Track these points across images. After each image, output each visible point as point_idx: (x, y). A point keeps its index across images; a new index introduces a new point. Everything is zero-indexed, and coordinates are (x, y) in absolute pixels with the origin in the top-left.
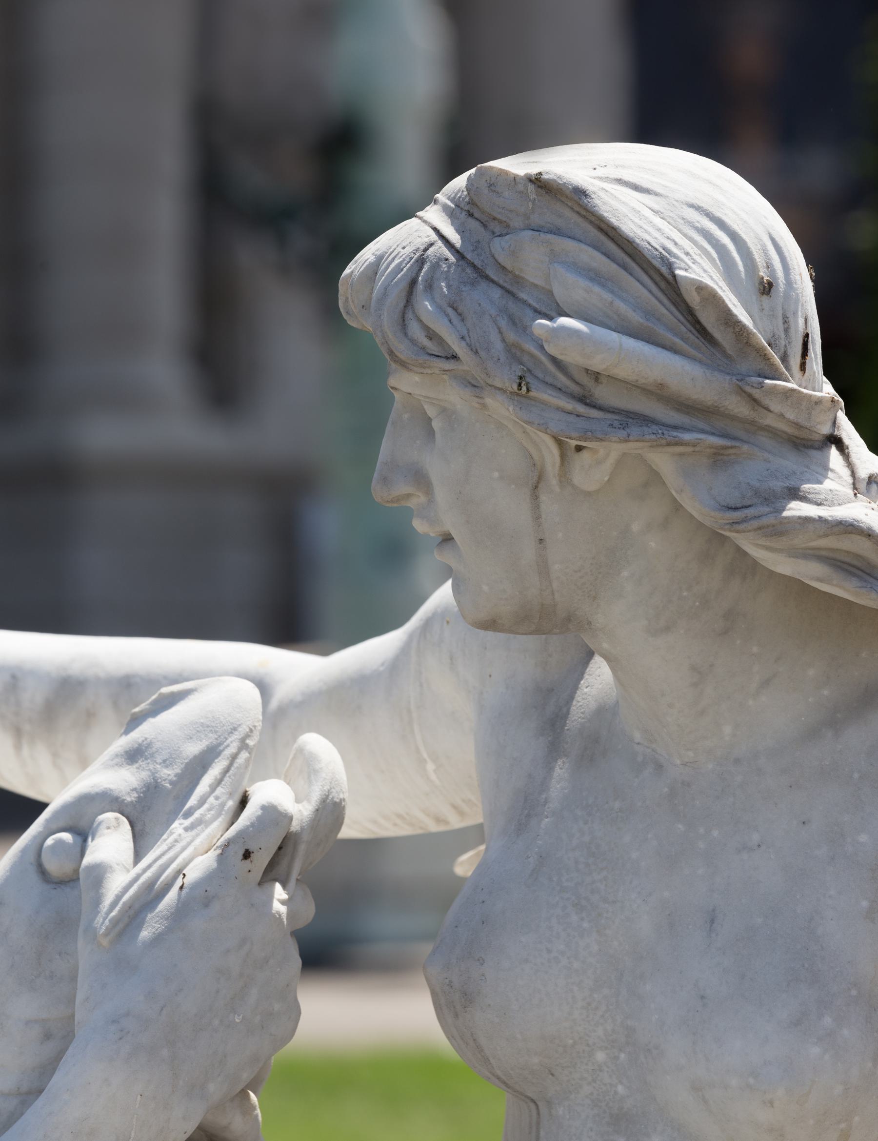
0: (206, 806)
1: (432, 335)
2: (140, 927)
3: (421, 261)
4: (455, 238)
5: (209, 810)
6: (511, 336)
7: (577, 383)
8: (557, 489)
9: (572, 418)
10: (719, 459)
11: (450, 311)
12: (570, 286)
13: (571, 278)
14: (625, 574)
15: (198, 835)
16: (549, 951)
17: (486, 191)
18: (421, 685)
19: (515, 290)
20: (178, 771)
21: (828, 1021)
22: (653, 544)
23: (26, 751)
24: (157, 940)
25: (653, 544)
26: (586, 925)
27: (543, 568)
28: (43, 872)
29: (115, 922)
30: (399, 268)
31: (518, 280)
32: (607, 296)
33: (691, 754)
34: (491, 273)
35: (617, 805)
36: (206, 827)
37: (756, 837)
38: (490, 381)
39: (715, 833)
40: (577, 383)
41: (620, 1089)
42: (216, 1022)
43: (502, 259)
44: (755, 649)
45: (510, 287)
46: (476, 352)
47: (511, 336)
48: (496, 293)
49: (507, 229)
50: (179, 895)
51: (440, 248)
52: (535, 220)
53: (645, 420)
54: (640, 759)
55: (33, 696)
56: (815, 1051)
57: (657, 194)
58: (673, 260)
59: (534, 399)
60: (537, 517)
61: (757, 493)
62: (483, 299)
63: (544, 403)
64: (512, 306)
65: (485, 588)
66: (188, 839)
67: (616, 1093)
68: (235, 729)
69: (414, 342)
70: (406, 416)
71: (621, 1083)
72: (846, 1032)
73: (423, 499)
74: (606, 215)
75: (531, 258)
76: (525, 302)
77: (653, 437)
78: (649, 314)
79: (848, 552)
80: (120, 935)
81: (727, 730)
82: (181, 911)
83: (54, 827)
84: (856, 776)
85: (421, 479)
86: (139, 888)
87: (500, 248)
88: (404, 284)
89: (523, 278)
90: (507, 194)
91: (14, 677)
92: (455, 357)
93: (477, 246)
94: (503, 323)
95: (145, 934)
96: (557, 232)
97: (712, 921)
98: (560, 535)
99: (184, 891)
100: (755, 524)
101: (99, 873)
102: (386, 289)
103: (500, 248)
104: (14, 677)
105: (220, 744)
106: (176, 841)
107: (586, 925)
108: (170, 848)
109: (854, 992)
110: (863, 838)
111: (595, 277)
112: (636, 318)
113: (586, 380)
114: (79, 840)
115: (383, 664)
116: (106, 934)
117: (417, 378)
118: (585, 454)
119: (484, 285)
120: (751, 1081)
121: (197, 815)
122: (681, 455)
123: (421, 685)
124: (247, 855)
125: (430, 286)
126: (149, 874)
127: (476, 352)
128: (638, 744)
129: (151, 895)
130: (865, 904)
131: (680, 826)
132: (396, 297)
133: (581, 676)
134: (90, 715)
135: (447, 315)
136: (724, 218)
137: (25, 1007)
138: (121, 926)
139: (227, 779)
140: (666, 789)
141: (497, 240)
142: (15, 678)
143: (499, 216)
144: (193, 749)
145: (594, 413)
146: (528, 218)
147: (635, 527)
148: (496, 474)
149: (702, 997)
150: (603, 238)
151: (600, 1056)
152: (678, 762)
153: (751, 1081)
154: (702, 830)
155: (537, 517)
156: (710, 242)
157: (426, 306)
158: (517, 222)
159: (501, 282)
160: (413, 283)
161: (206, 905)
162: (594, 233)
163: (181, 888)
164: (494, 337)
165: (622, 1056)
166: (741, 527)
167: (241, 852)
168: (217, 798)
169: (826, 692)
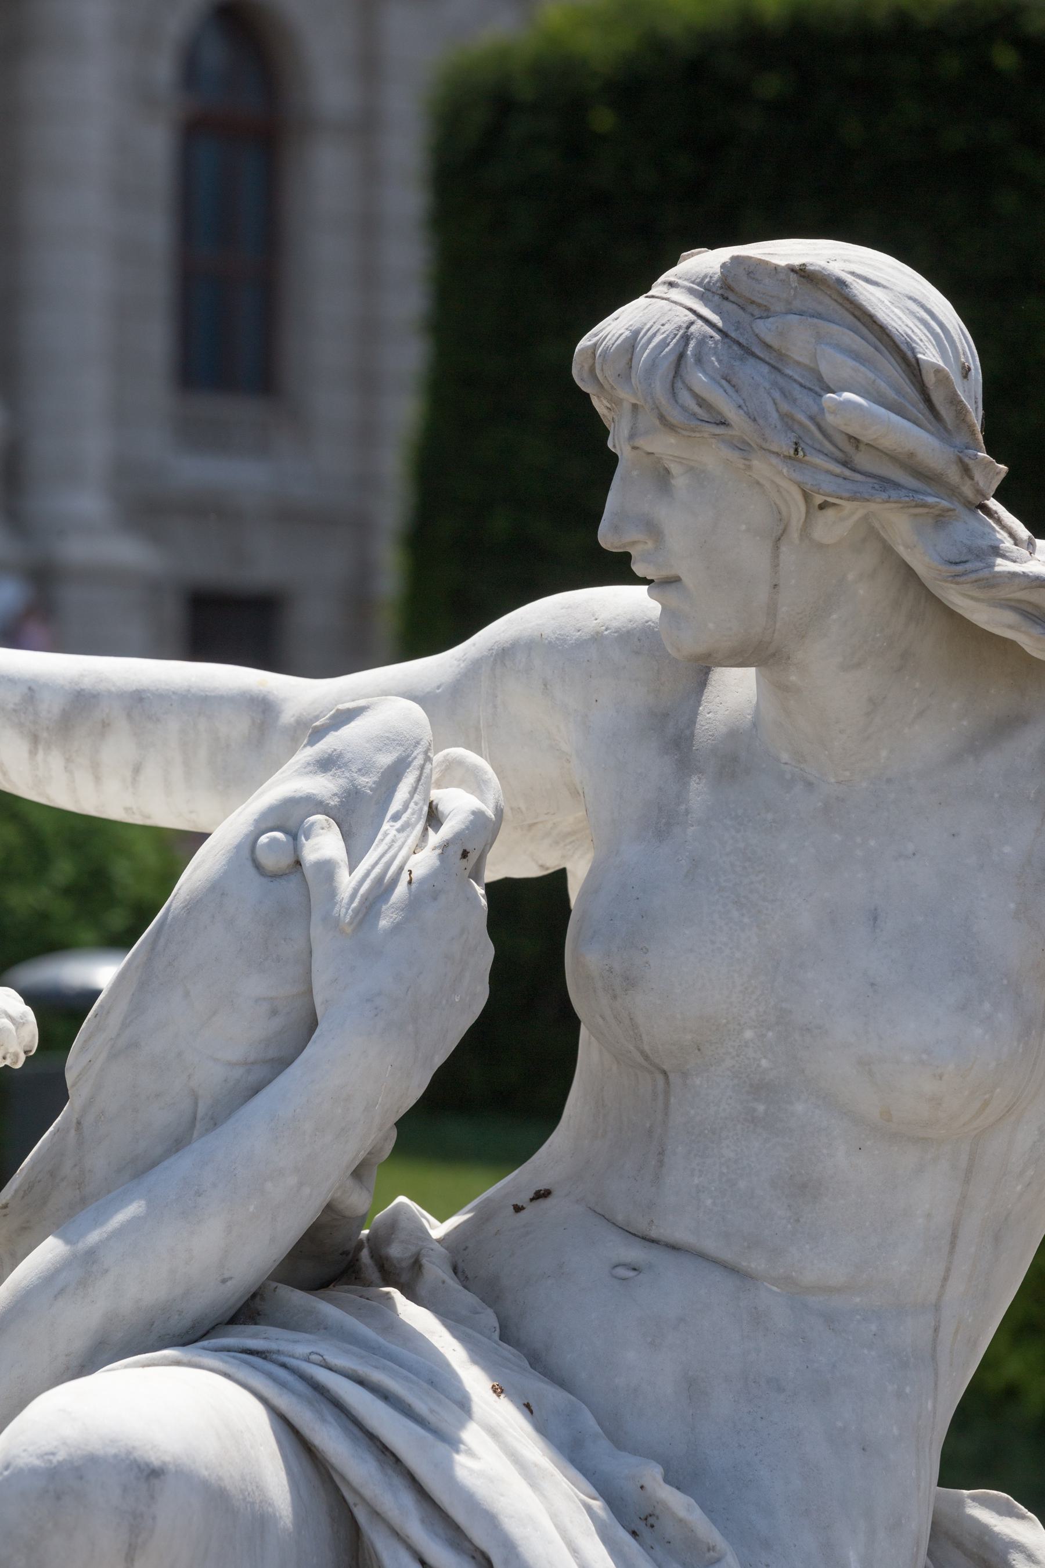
0: (409, 811)
1: (701, 402)
2: (378, 916)
3: (686, 338)
4: (715, 318)
5: (413, 814)
6: (785, 407)
7: (841, 450)
8: (797, 541)
9: (840, 481)
10: (941, 519)
11: (724, 382)
12: (833, 364)
13: (840, 357)
14: (834, 616)
15: (408, 836)
16: (713, 942)
17: (745, 278)
18: (495, 707)
19: (779, 365)
20: (375, 779)
21: (987, 1006)
22: (861, 592)
23: (40, 755)
24: (396, 929)
25: (861, 592)
26: (746, 920)
27: (772, 610)
28: (257, 866)
29: (357, 912)
30: (664, 343)
31: (781, 356)
32: (871, 375)
33: (848, 774)
34: (757, 351)
35: (770, 816)
36: (413, 829)
37: (911, 847)
38: (765, 445)
39: (872, 843)
40: (841, 450)
41: (764, 1063)
42: (444, 1002)
43: (769, 339)
44: (917, 685)
45: (775, 361)
46: (755, 420)
47: (785, 407)
48: (766, 369)
49: (766, 313)
50: (409, 889)
51: (699, 326)
52: (797, 304)
53: (897, 486)
54: (788, 776)
55: (50, 707)
56: (979, 1031)
57: (884, 287)
58: (914, 345)
59: (807, 463)
60: (775, 566)
61: (970, 550)
62: (752, 373)
63: (815, 467)
64: (781, 380)
65: (711, 626)
66: (402, 840)
67: (759, 1066)
68: (418, 743)
69: (684, 409)
70: (635, 473)
71: (765, 1057)
72: (1000, 1015)
73: (650, 545)
74: (864, 303)
75: (799, 341)
76: (790, 377)
77: (907, 499)
78: (898, 391)
79: (1029, 603)
80: (361, 923)
81: (884, 753)
82: (414, 903)
83: (263, 826)
84: (996, 795)
85: (654, 530)
86: (373, 882)
87: (765, 329)
88: (673, 358)
89: (787, 356)
90: (767, 281)
91: (30, 688)
92: (724, 423)
93: (738, 326)
94: (777, 395)
95: (384, 923)
96: (819, 316)
97: (875, 919)
98: (793, 582)
99: (414, 886)
100: (974, 576)
101: (327, 868)
102: (654, 361)
103: (765, 329)
104: (30, 688)
105: (408, 756)
106: (393, 841)
107: (746, 920)
108: (390, 847)
109: (1005, 982)
110: (1007, 849)
111: (856, 356)
112: (891, 394)
113: (849, 448)
114: (290, 838)
115: (438, 687)
116: (350, 923)
117: (673, 441)
118: (830, 513)
119: (751, 361)
120: (924, 1057)
121: (404, 817)
122: (916, 515)
123: (495, 707)
124: (465, 854)
125: (699, 360)
126: (377, 870)
127: (755, 420)
128: (786, 764)
129: (382, 889)
130: (1012, 906)
131: (836, 836)
132: (665, 367)
134: (105, 725)
135: (722, 386)
136: (933, 310)
137: (256, 986)
138: (361, 916)
139: (420, 787)
140: (820, 804)
141: (760, 322)
142: (31, 691)
143: (760, 301)
144: (385, 759)
145: (858, 477)
146: (790, 303)
147: (851, 577)
148: (743, 527)
149: (872, 984)
150: (858, 324)
151: (749, 1034)
152: (833, 780)
153: (924, 1057)
154: (859, 840)
155: (775, 566)
156: (929, 331)
157: (699, 379)
158: (779, 307)
159: (767, 359)
160: (681, 356)
161: (435, 898)
162: (850, 318)
163: (410, 882)
164: (770, 407)
165: (770, 1034)
166: (962, 579)
167: (460, 852)
168: (416, 804)
169: (965, 723)
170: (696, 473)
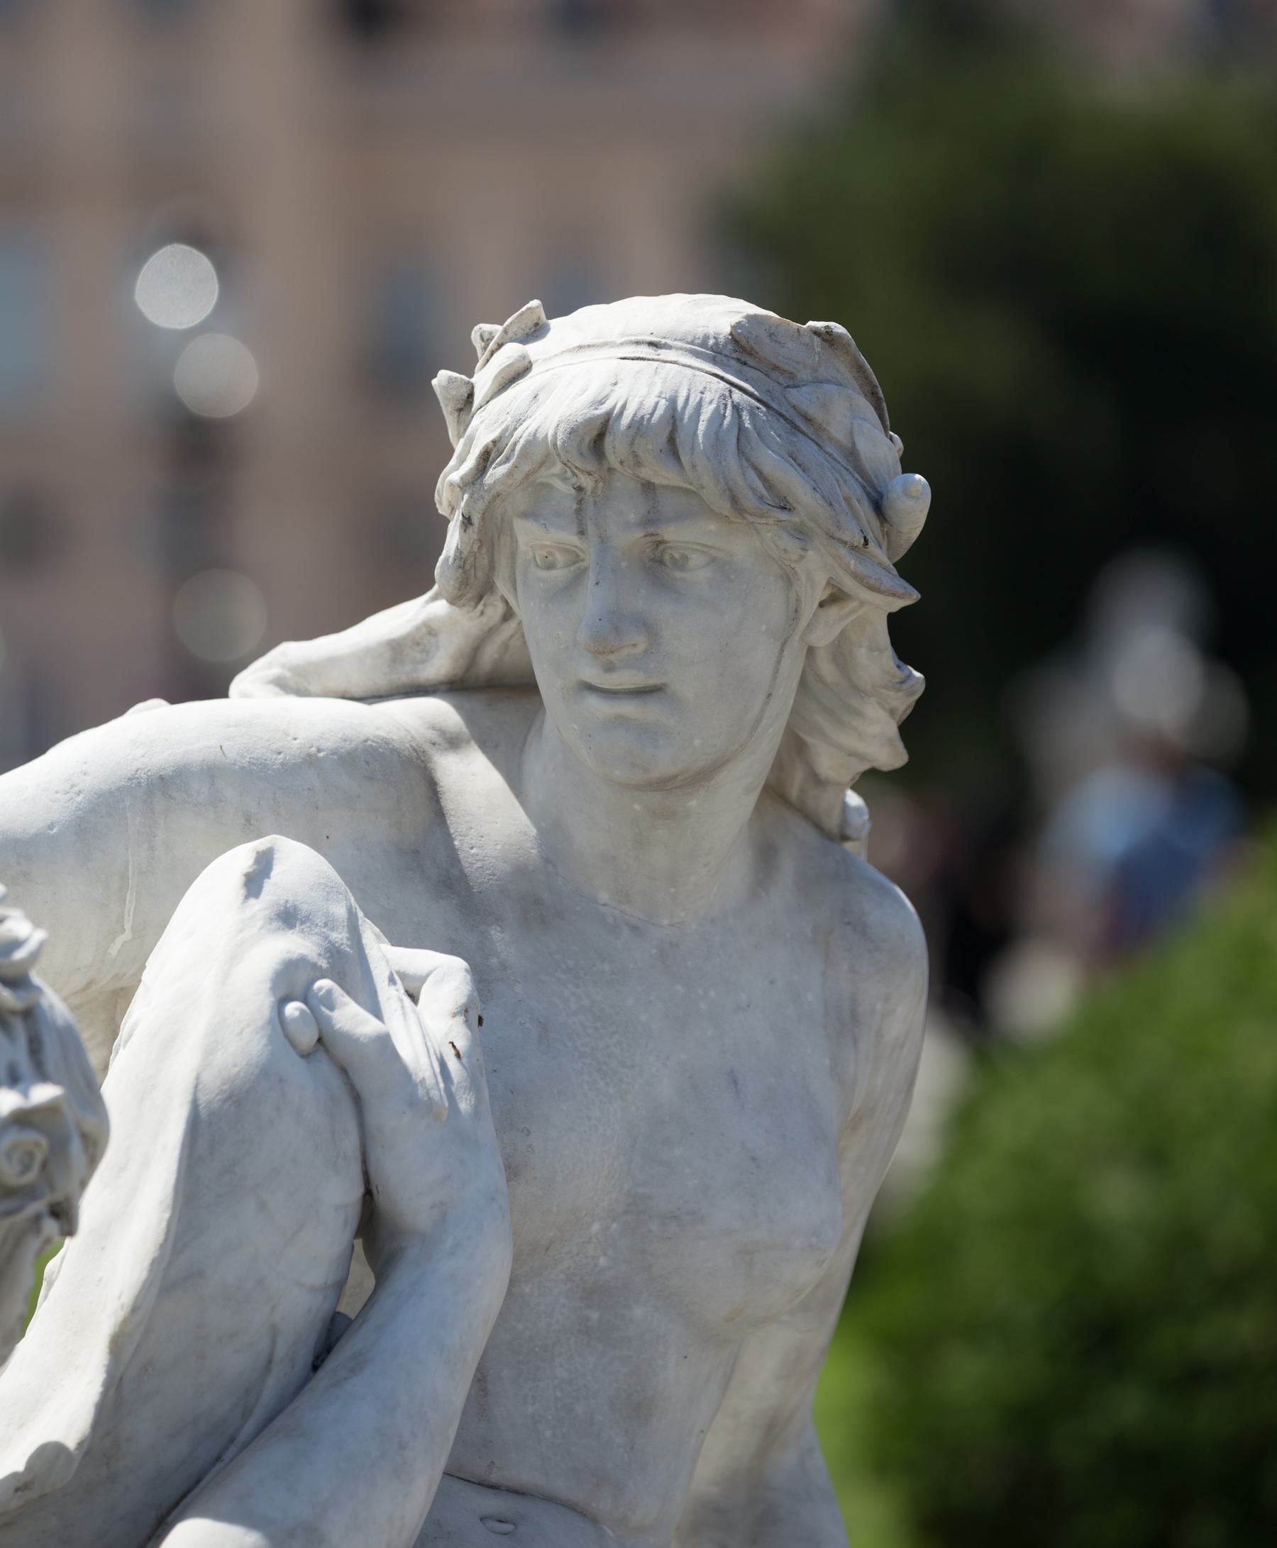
3: (737, 408)
16: (589, 1119)
17: (767, 340)
26: (611, 1091)
30: (718, 416)
33: (683, 914)
35: (607, 967)
38: (838, 534)
39: (712, 994)
41: (602, 1261)
46: (831, 505)
51: (737, 395)
54: (610, 920)
65: (697, 742)
70: (624, 564)
71: (605, 1254)
87: (803, 398)
89: (824, 430)
90: (789, 345)
97: (735, 1083)
99: (464, 1060)
115: (51, 827)
120: (814, 1240)
123: (152, 849)
127: (831, 505)
128: (605, 905)
133: (449, 838)
141: (793, 391)
143: (786, 367)
146: (816, 371)
148: (764, 628)
151: (596, 1227)
152: (666, 922)
154: (700, 991)
158: (804, 375)
163: (458, 1055)
165: (614, 1226)
170: (723, 567)
